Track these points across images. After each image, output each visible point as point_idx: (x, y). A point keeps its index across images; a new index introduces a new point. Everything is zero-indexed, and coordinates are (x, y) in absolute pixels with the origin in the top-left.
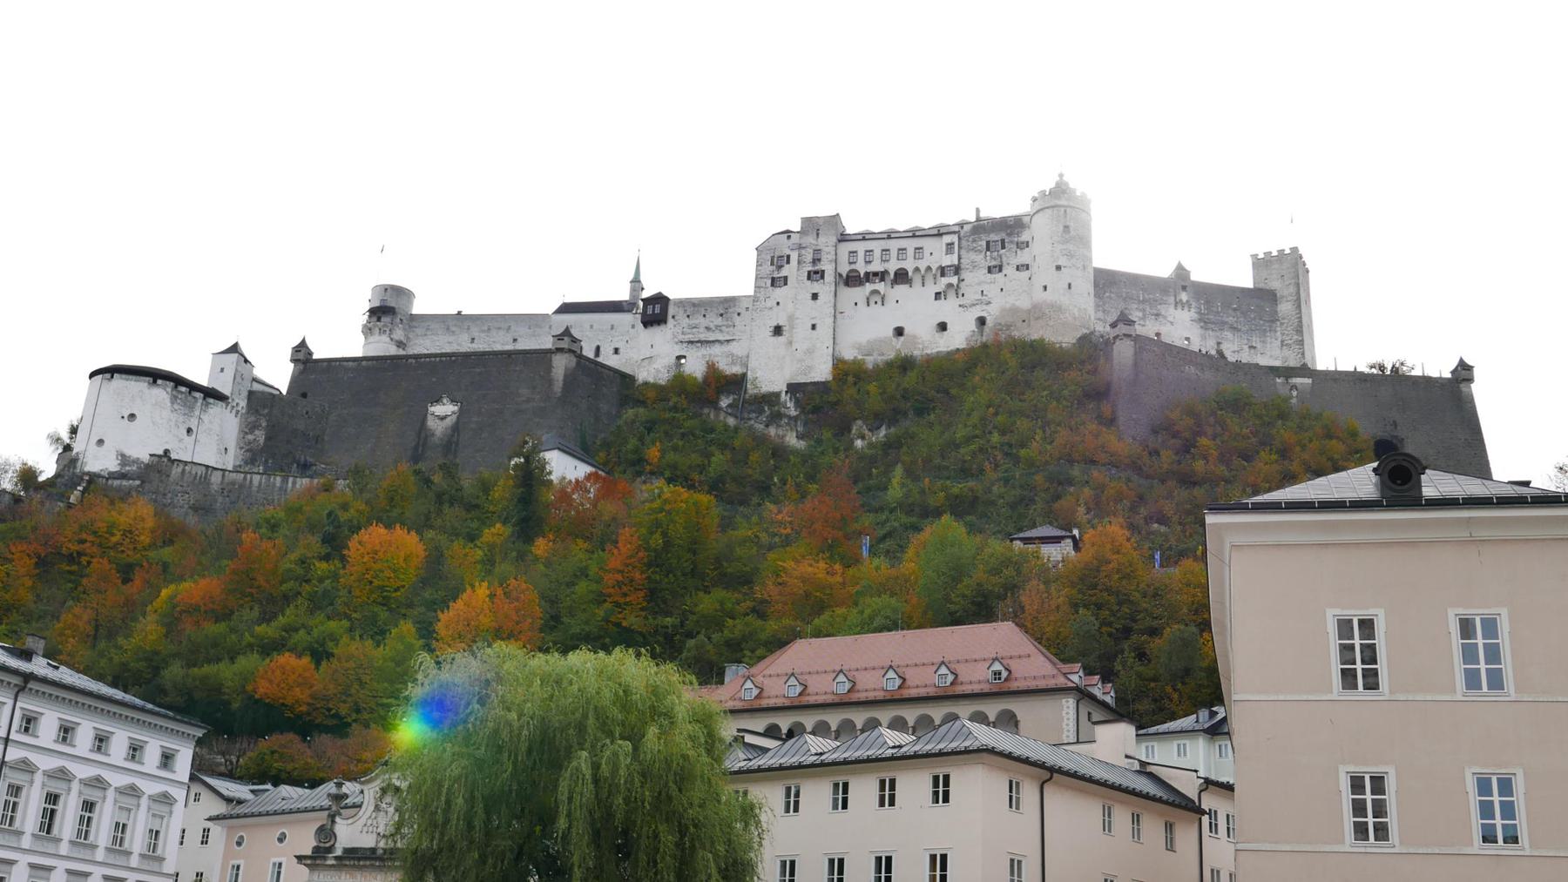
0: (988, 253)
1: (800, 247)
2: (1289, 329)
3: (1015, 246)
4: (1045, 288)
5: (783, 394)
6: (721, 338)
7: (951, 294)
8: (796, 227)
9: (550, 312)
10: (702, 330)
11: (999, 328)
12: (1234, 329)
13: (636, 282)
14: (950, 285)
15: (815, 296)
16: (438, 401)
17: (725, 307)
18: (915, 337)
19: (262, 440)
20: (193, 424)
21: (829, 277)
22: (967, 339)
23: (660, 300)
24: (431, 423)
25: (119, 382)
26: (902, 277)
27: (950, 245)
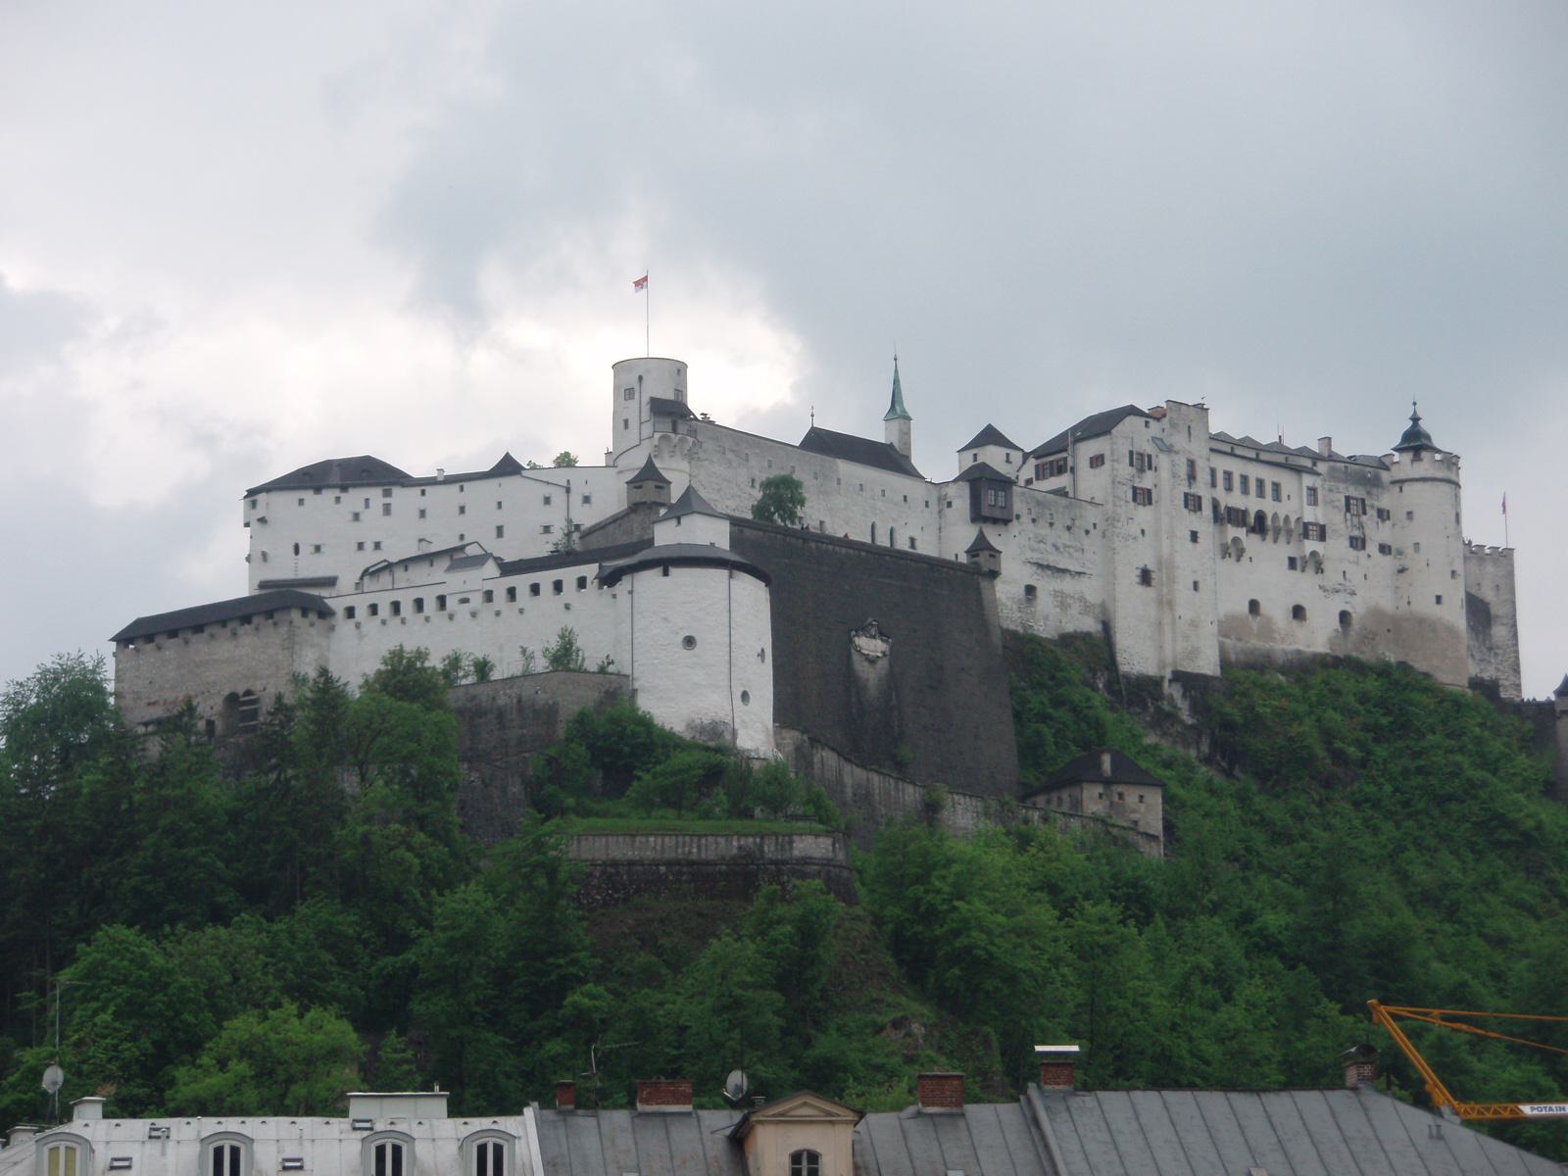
0: (1348, 515)
1: (1169, 450)
2: (1505, 664)
3: (1375, 514)
4: (1439, 599)
5: (1166, 684)
6: (1071, 568)
7: (1310, 570)
10: (1050, 549)
11: (1368, 637)
14: (1314, 554)
15: (1194, 536)
16: (863, 630)
18: (1269, 620)
22: (1329, 639)
26: (1259, 526)
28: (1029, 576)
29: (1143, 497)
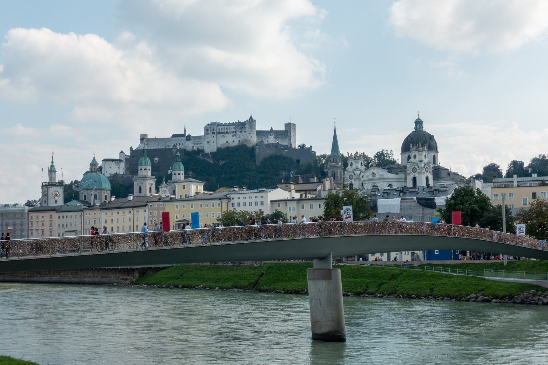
5: (210, 154)
8: (210, 123)
9: (170, 137)
11: (242, 142)
12: (280, 138)
13: (185, 131)
15: (213, 137)
16: (155, 158)
17: (200, 137)
18: (229, 143)
19: (128, 166)
20: (119, 166)
21: (215, 133)
23: (189, 136)
24: (155, 161)
25: (108, 162)
26: (227, 133)
27: (234, 127)
28: (193, 145)
29: (208, 134)
